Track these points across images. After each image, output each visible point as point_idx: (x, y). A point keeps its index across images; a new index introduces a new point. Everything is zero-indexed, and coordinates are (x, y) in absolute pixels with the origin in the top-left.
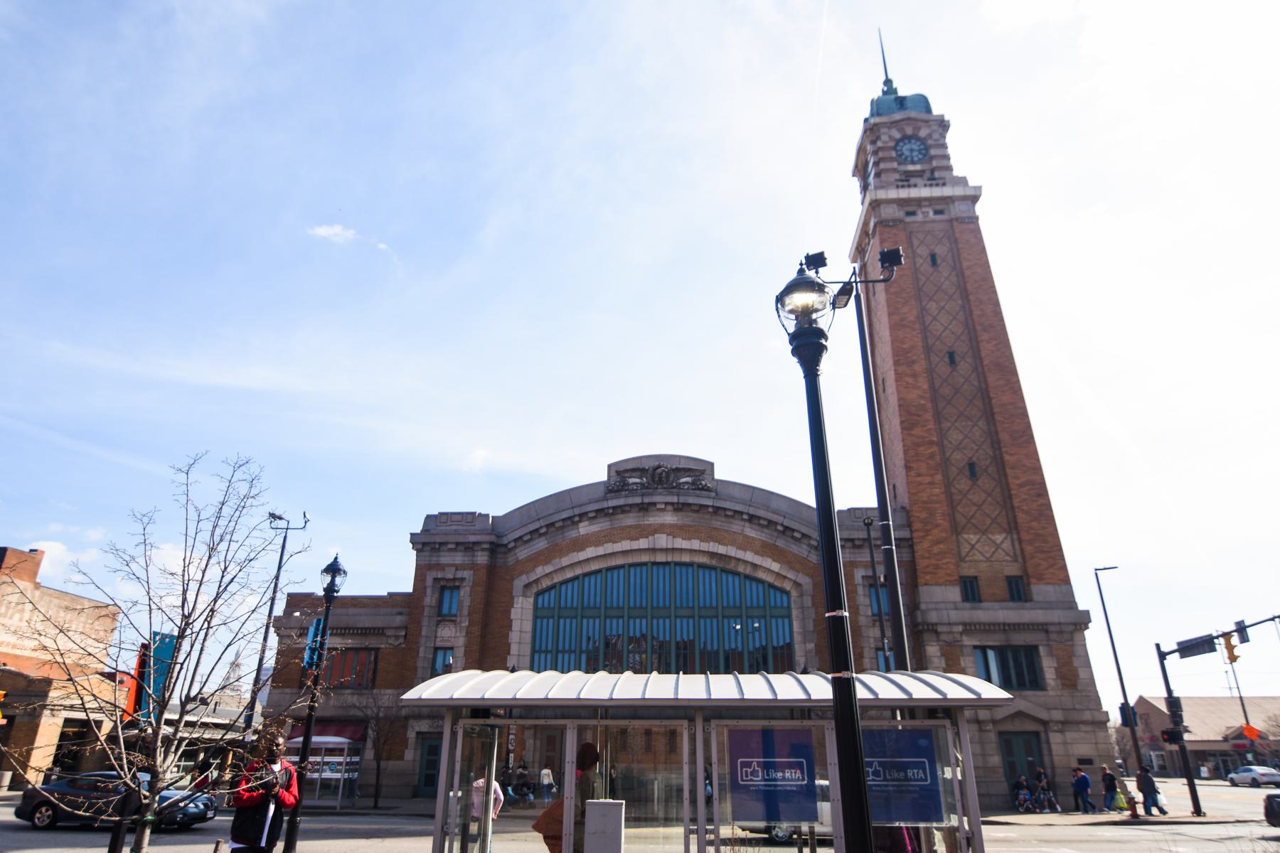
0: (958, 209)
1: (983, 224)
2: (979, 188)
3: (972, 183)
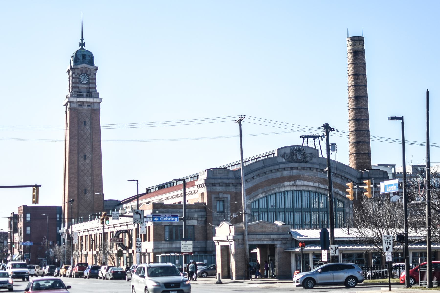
0: (95, 106)
1: (101, 112)
2: (102, 99)
3: (100, 97)
